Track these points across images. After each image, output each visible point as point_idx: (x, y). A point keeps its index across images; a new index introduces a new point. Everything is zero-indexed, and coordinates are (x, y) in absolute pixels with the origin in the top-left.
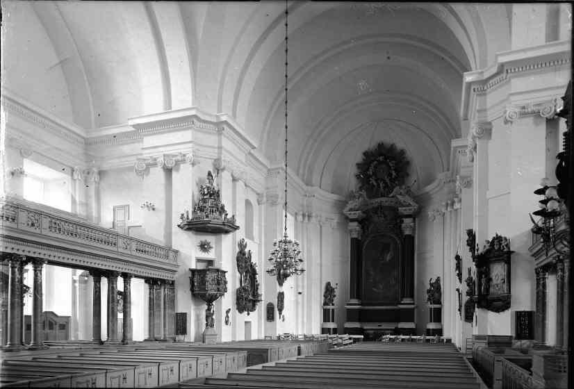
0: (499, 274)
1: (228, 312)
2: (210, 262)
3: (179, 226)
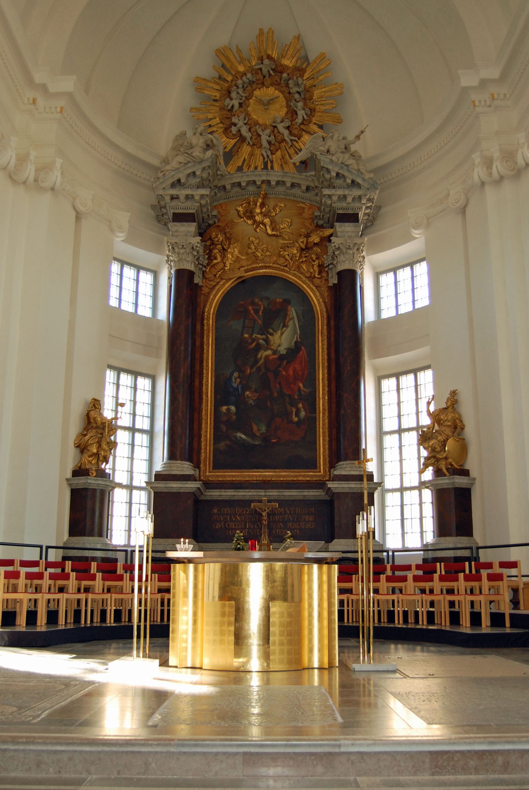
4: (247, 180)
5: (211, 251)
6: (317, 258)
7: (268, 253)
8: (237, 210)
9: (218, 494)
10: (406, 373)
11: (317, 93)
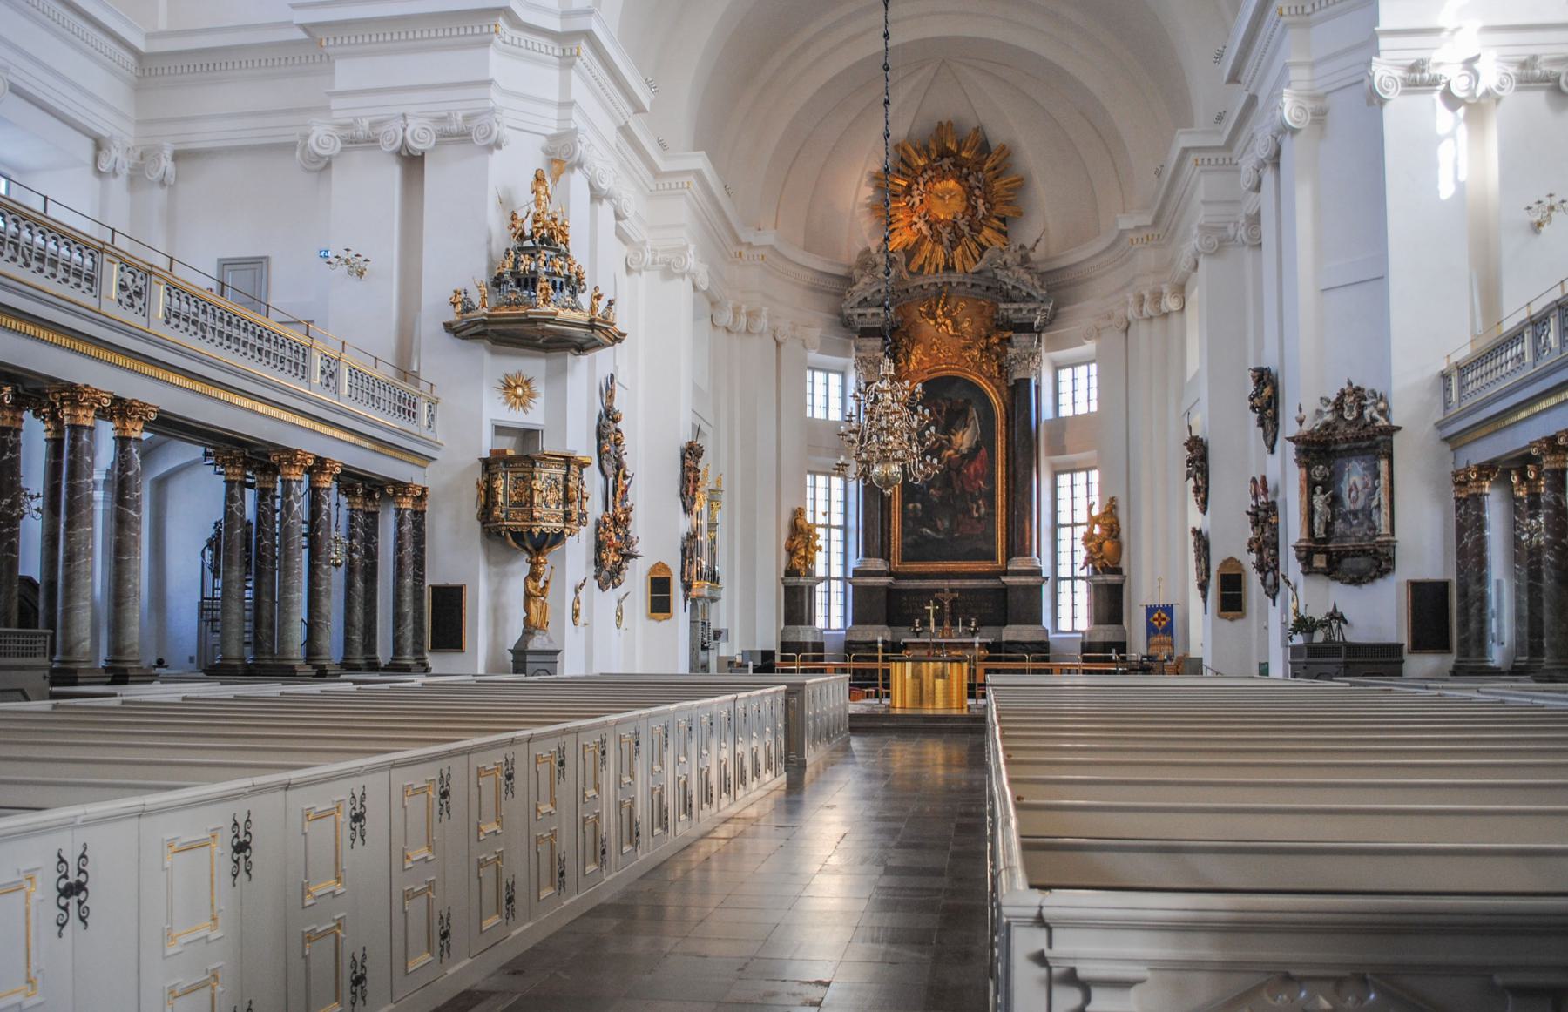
2: (529, 435)
3: (448, 327)
6: (998, 358)
7: (950, 354)
10: (1080, 470)
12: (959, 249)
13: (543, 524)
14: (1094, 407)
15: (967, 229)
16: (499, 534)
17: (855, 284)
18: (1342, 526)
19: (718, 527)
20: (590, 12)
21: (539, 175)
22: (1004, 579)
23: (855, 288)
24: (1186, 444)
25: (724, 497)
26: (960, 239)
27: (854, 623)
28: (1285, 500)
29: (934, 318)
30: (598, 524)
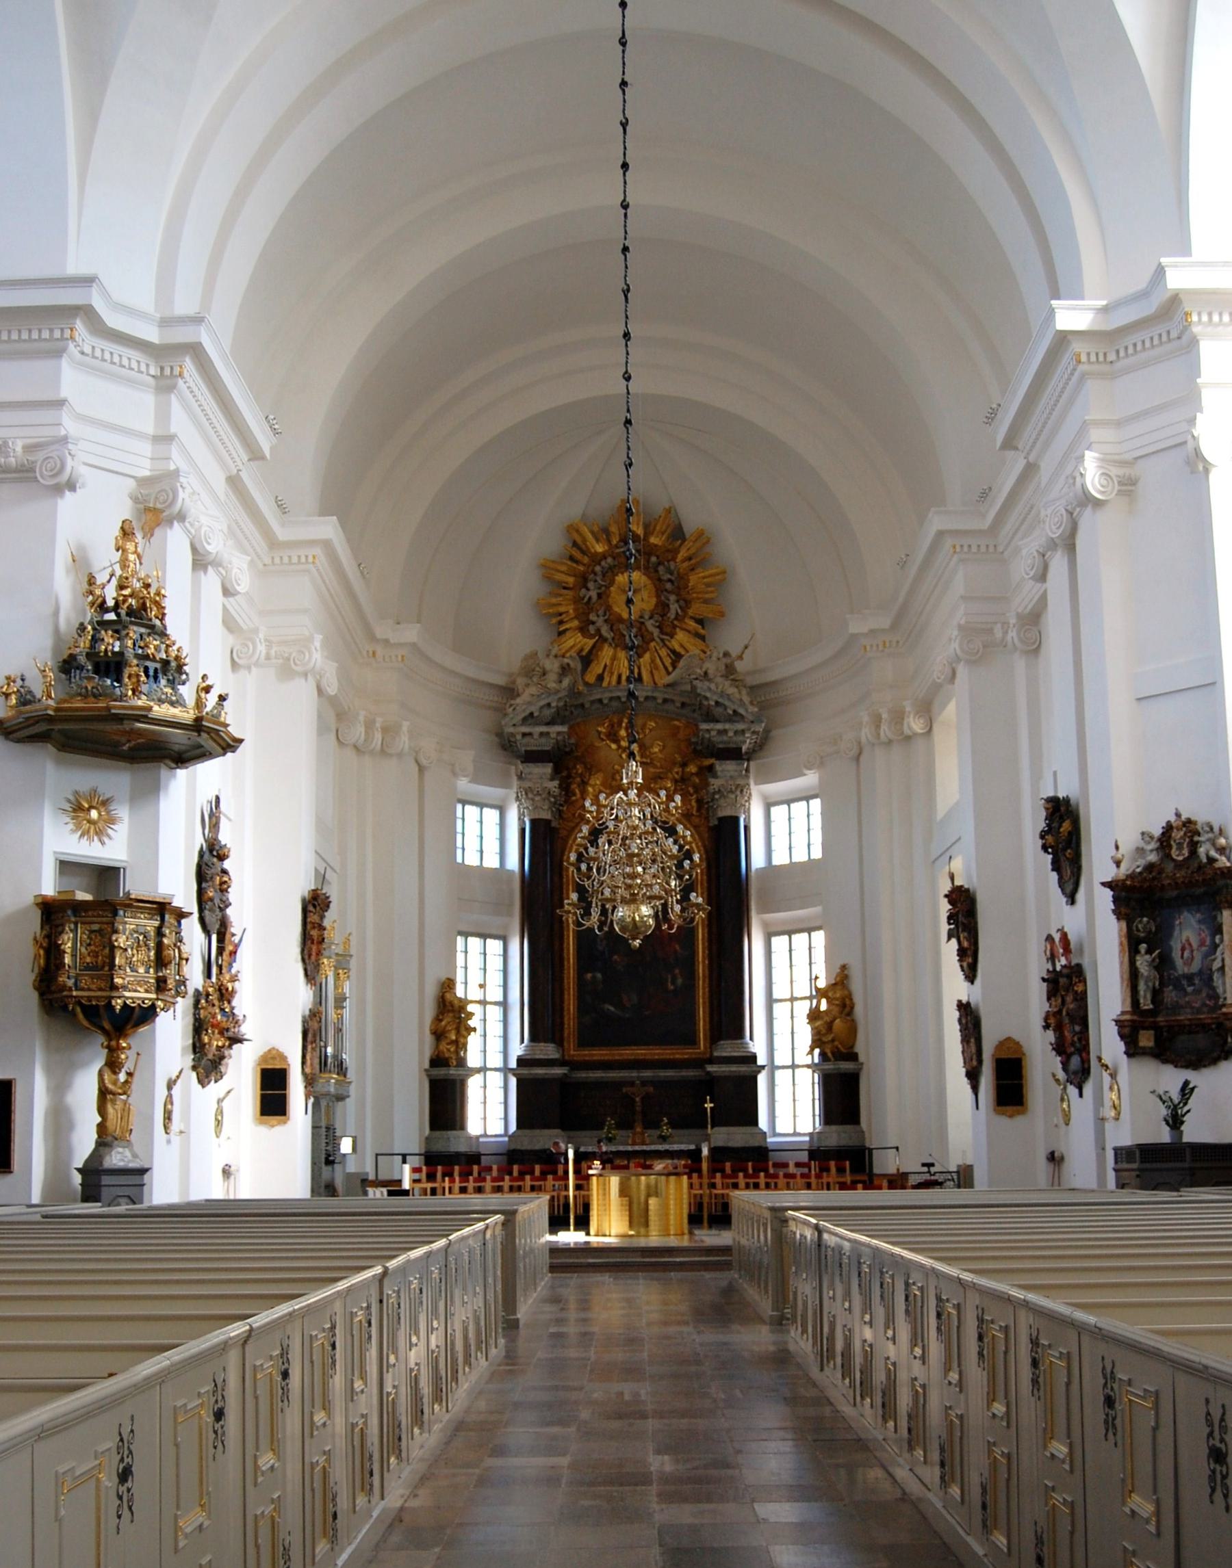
0: (1195, 945)
1: (170, 1085)
2: (107, 875)
4: (611, 695)
5: (568, 785)
6: (696, 792)
8: (598, 731)
9: (584, 1075)
11: (693, 579)
12: (647, 656)
13: (127, 994)
14: (817, 854)
15: (656, 632)
16: (65, 1008)
17: (518, 695)
18: (1173, 994)
19: (347, 1003)
20: (198, 320)
21: (126, 527)
22: (710, 1068)
23: (518, 701)
24: (946, 896)
25: (353, 964)
26: (648, 643)
27: (519, 1126)
28: (1095, 964)
29: (616, 740)
30: (197, 994)
